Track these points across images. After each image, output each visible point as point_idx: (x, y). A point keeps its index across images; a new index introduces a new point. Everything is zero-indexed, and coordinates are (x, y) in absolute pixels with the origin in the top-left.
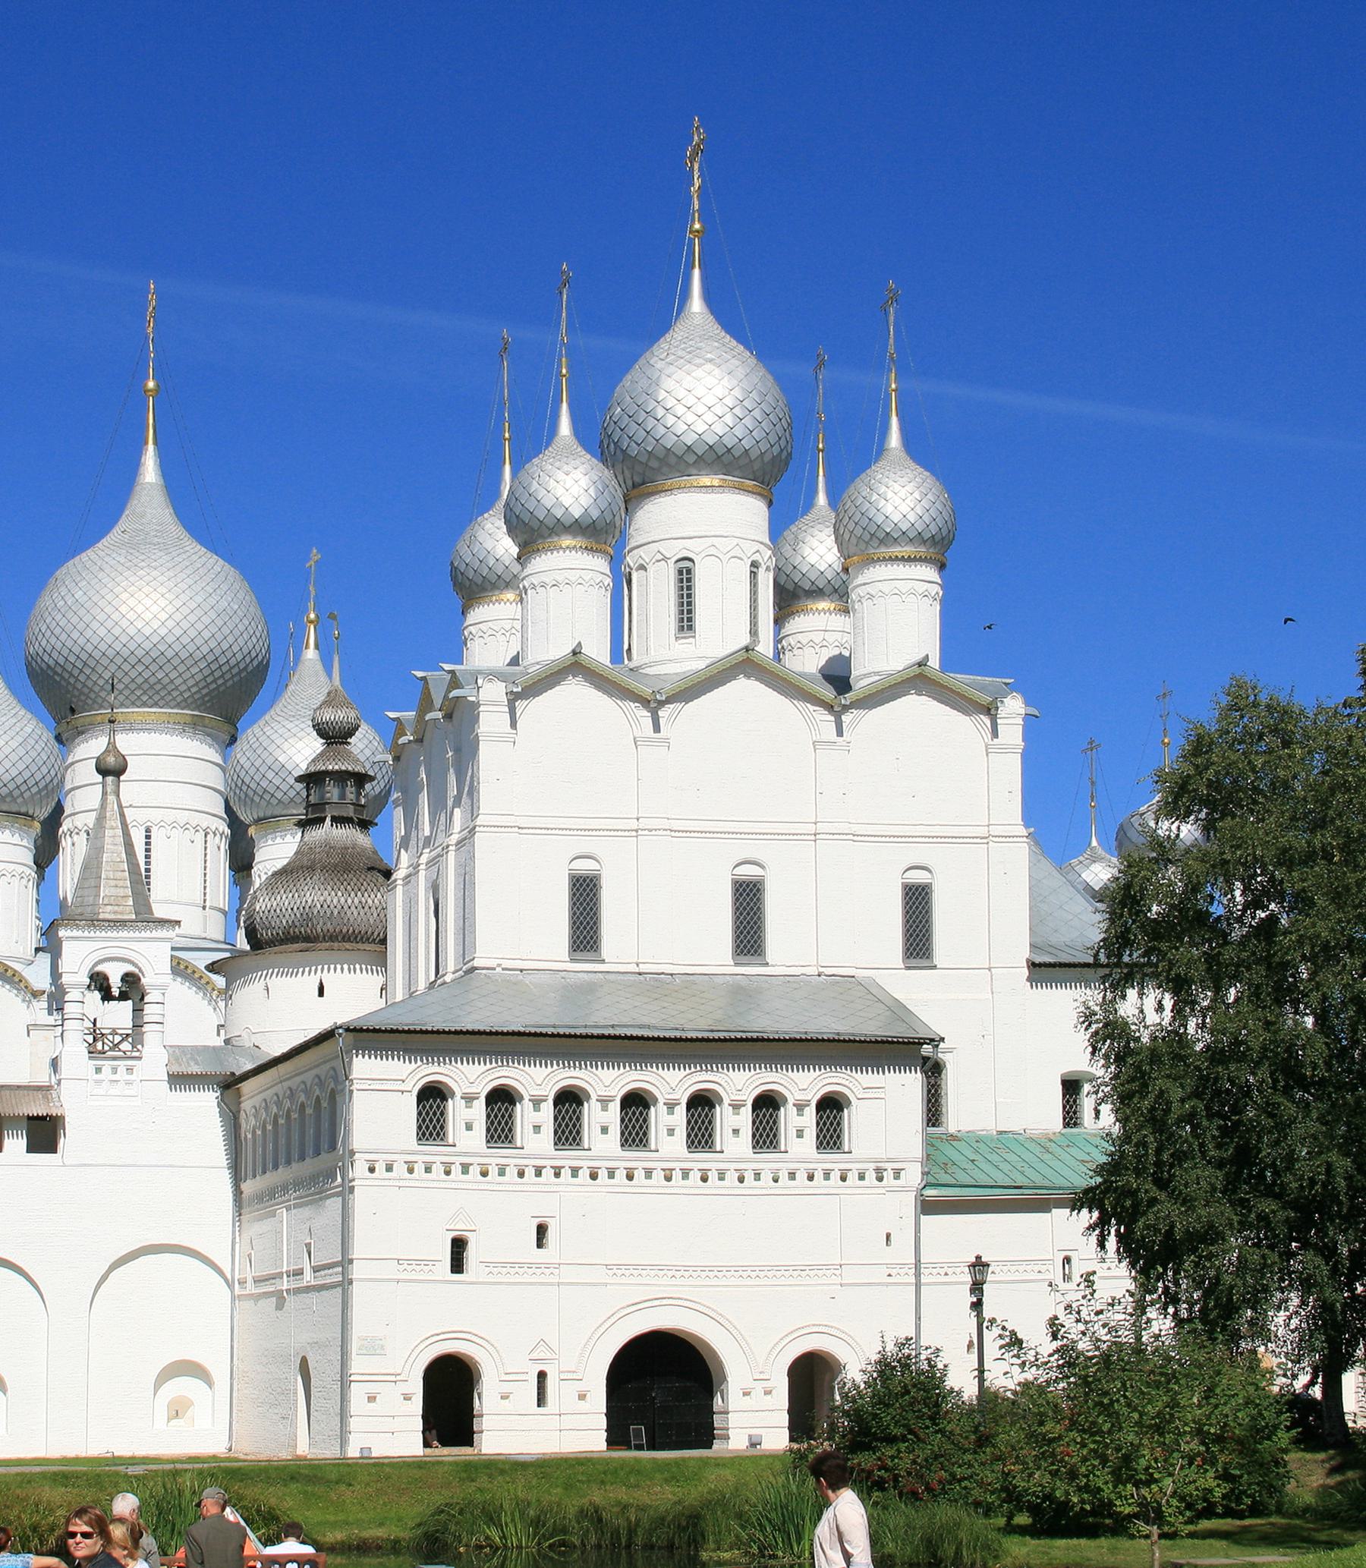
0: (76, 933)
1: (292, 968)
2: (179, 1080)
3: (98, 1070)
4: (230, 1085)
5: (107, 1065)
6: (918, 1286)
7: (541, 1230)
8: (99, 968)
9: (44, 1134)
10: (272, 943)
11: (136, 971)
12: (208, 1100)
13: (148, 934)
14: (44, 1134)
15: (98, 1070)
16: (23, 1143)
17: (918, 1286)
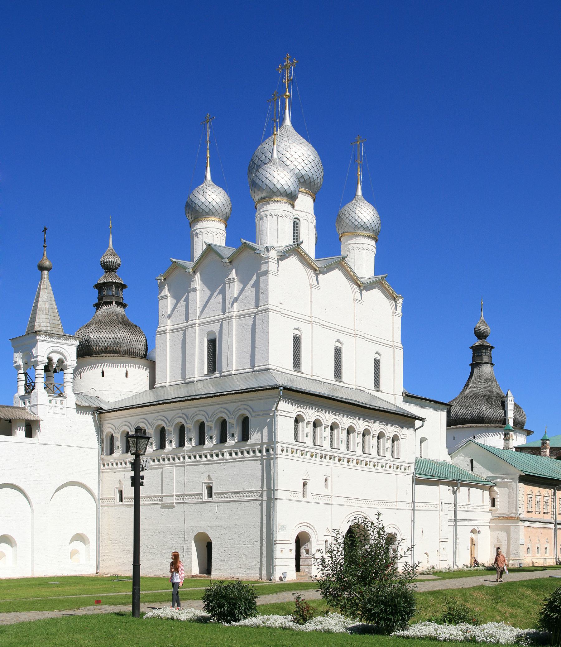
0: (44, 338)
1: (116, 364)
2: (80, 408)
3: (50, 401)
4: (99, 412)
5: (54, 399)
6: (413, 510)
7: (326, 480)
8: (50, 355)
9: (31, 428)
10: (97, 353)
11: (63, 358)
12: (88, 419)
13: (69, 342)
14: (31, 428)
15: (50, 401)
16: (24, 433)
17: (413, 510)
